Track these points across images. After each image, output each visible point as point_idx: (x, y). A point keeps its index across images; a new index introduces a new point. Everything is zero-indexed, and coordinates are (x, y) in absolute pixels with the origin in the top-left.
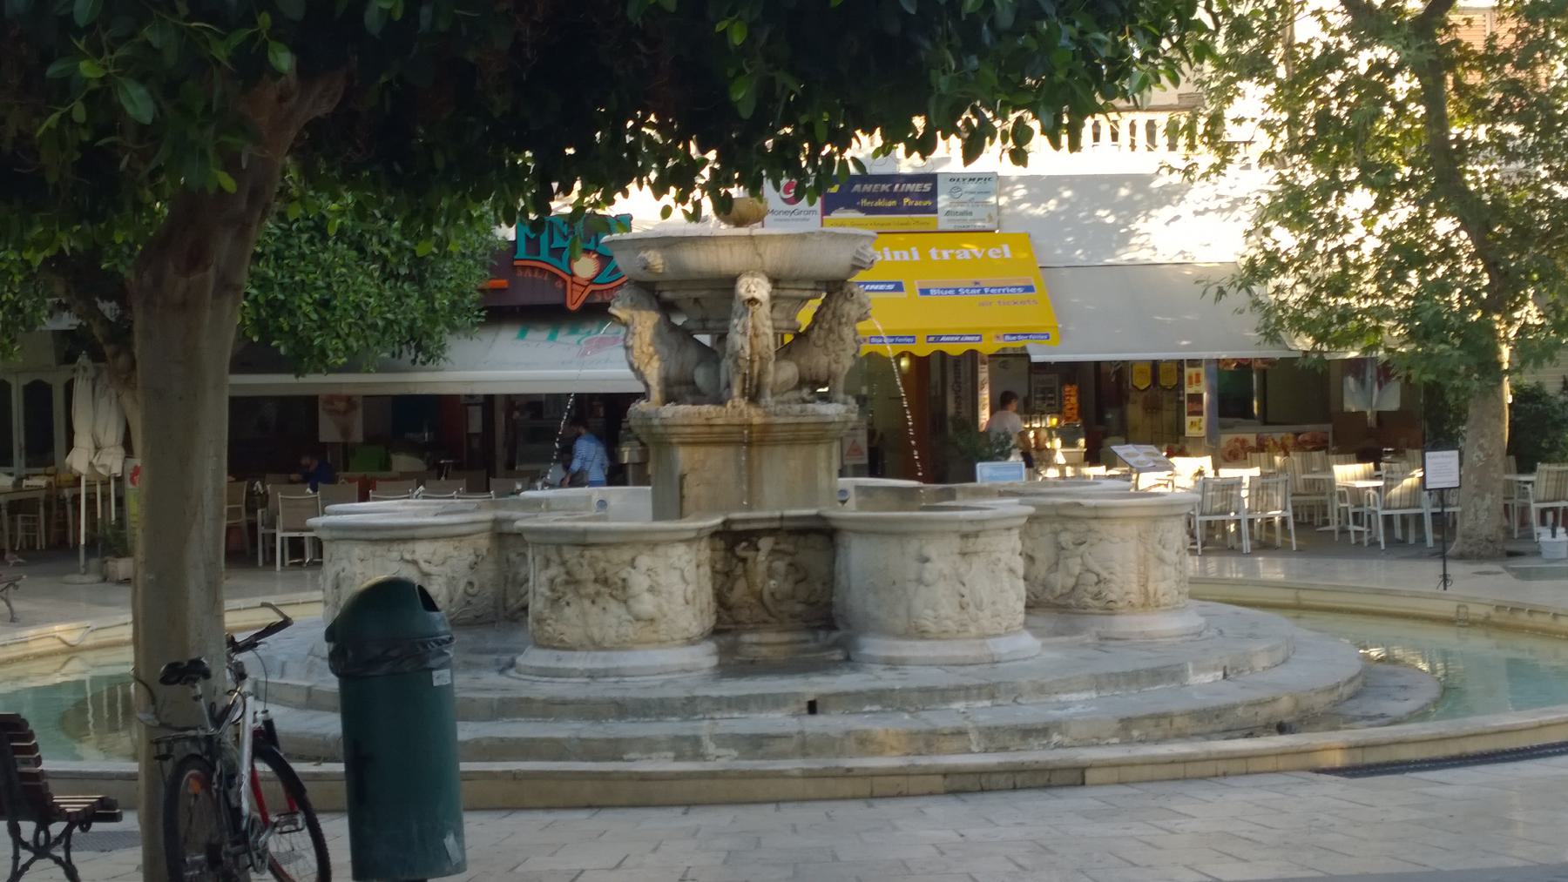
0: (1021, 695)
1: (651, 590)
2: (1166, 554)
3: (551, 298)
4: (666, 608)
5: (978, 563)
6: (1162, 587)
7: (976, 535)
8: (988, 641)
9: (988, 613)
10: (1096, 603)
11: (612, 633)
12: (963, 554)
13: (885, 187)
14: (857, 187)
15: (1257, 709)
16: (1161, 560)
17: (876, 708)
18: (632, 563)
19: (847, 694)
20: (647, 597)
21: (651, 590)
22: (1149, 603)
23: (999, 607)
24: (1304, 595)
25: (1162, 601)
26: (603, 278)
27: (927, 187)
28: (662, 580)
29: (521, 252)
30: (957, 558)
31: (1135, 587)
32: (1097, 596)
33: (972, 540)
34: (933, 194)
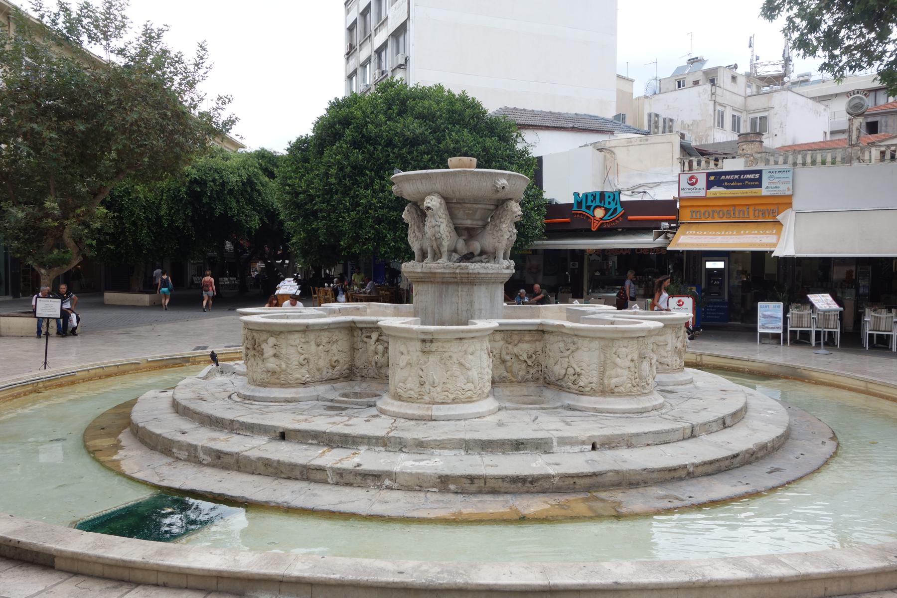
0: (405, 446)
1: (275, 355)
2: (618, 360)
3: (586, 226)
4: (284, 366)
5: (433, 359)
6: (614, 381)
7: (432, 341)
8: (434, 406)
9: (439, 389)
10: (573, 387)
11: (259, 378)
12: (424, 352)
13: (737, 177)
14: (723, 177)
15: (576, 480)
16: (616, 365)
17: (315, 442)
18: (266, 341)
19: (299, 431)
20: (272, 359)
21: (275, 355)
22: (606, 391)
23: (448, 386)
24: (870, 386)
25: (616, 390)
26: (606, 218)
27: (757, 176)
28: (284, 351)
29: (575, 208)
30: (420, 354)
31: (595, 379)
32: (574, 383)
33: (428, 344)
34: (760, 180)
